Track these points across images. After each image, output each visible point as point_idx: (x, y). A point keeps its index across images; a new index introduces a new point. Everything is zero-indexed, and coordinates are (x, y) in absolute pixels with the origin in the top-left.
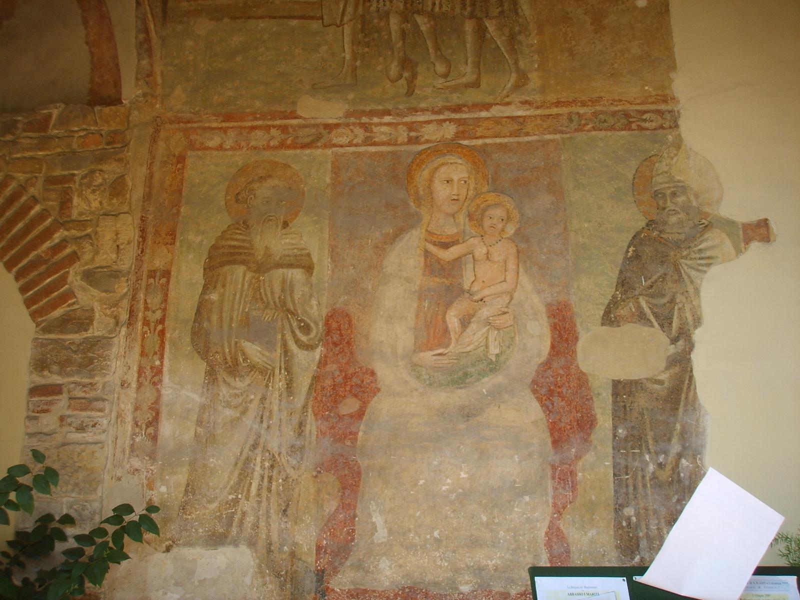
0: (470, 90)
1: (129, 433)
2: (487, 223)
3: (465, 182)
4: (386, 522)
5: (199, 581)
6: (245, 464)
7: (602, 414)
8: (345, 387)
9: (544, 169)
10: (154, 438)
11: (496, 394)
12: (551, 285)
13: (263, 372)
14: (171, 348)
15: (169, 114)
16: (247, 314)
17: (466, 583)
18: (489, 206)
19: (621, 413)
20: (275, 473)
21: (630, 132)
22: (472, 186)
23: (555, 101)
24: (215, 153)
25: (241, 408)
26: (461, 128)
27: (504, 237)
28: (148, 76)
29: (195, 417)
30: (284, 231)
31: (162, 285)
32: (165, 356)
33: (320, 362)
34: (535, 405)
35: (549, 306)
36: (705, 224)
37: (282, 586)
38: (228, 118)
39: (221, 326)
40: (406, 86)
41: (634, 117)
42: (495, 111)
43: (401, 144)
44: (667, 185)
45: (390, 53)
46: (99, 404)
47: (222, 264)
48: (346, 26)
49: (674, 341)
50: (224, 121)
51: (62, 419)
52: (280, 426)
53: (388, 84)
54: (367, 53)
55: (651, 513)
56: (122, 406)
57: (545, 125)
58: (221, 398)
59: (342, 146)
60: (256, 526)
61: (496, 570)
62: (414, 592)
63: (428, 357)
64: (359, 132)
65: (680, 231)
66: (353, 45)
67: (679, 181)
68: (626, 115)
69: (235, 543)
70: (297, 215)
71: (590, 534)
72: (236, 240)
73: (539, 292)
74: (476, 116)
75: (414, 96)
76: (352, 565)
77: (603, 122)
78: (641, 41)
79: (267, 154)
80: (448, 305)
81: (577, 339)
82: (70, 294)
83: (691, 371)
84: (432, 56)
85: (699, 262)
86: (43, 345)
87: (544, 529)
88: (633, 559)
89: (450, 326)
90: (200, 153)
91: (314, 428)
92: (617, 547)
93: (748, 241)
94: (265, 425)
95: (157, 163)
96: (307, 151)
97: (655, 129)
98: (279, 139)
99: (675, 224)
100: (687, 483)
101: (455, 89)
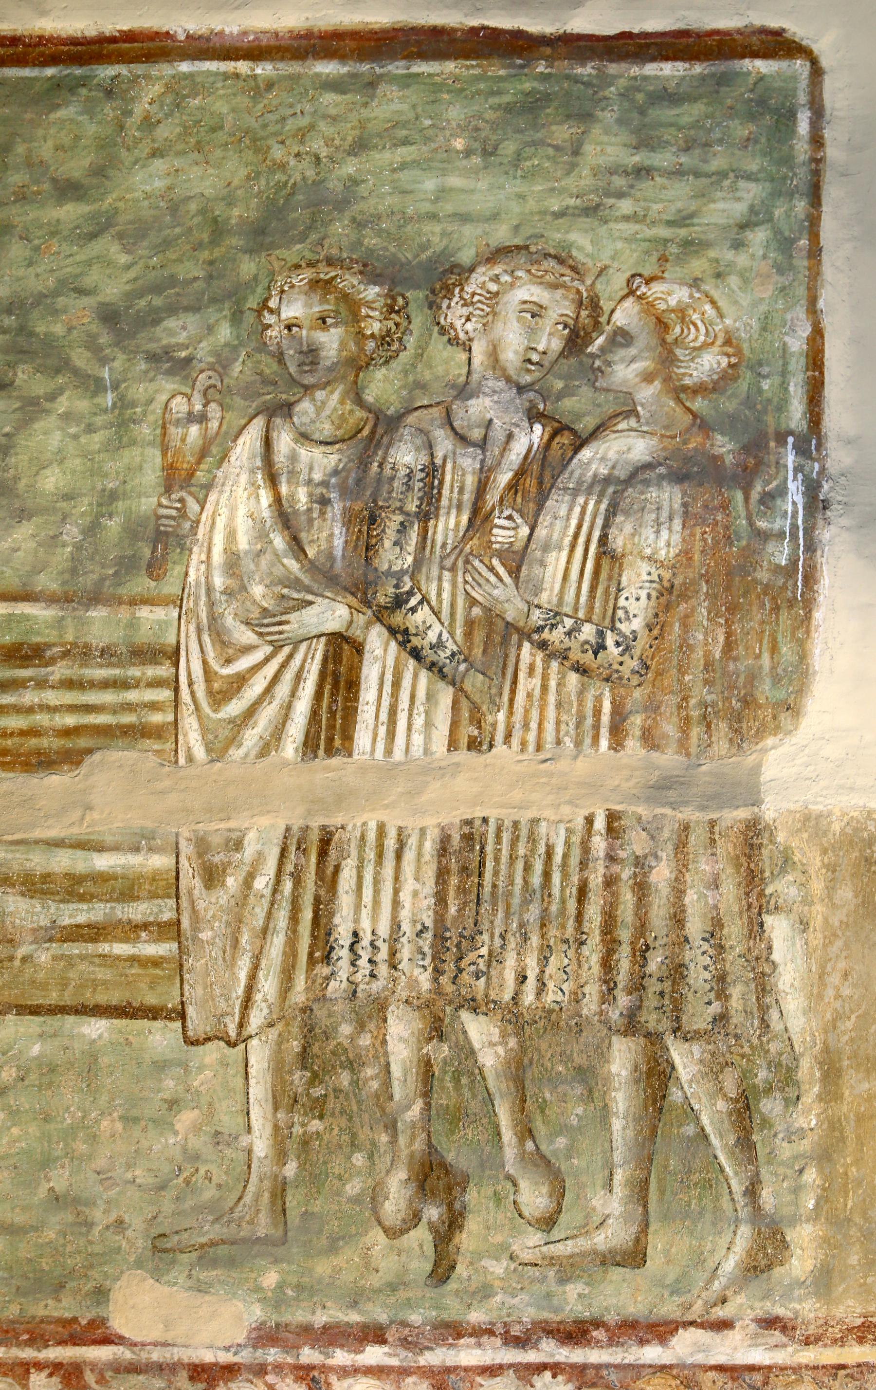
40: (429, 1249)
48: (254, 1042)
53: (377, 1237)
66: (276, 1108)
75: (452, 1285)
84: (510, 1153)
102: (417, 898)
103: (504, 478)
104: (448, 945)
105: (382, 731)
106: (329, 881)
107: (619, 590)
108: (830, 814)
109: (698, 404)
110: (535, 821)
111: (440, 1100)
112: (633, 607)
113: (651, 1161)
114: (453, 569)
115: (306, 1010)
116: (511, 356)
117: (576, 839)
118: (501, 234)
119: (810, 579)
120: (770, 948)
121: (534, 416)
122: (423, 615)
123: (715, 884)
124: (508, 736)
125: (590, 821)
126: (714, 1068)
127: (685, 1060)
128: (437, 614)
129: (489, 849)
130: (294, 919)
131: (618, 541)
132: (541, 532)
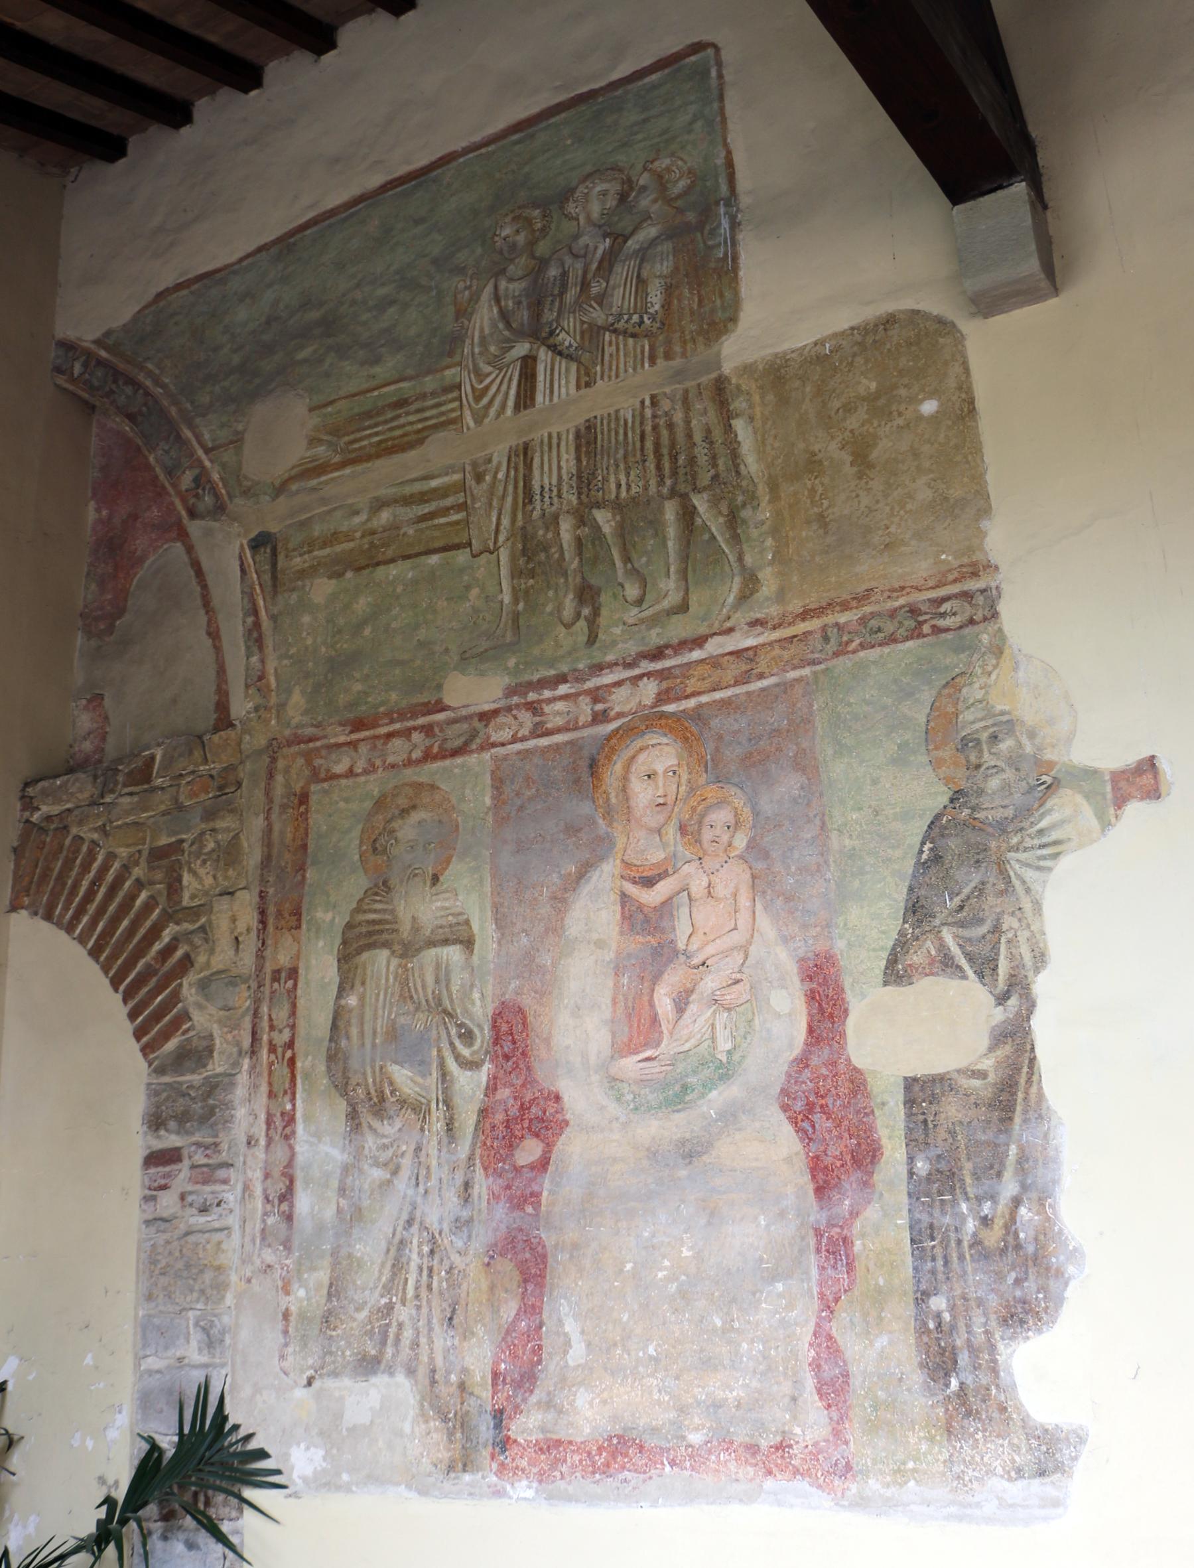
0: (675, 618)
1: (260, 1213)
2: (707, 835)
3: (674, 773)
4: (583, 1332)
5: (347, 1430)
6: (399, 1249)
7: (890, 1138)
8: (523, 1124)
9: (788, 731)
10: (289, 1218)
11: (730, 1116)
12: (805, 926)
13: (416, 1109)
14: (303, 1084)
15: (287, 732)
16: (394, 1022)
17: (697, 1429)
18: (708, 808)
19: (920, 1130)
20: (435, 1262)
21: (920, 641)
22: (685, 777)
23: (801, 610)
24: (344, 782)
25: (392, 1166)
26: (665, 685)
27: (732, 855)
28: (260, 678)
29: (335, 1184)
30: (434, 890)
31: (288, 991)
32: (298, 1096)
33: (487, 1088)
34: (788, 1129)
35: (802, 960)
36: (1046, 783)
37: (451, 1434)
38: (358, 725)
39: (363, 1045)
40: (586, 630)
41: (926, 613)
42: (713, 647)
43: (584, 727)
44: (982, 724)
45: (562, 580)
46: (222, 1173)
47: (359, 951)
49: (1002, 999)
50: (352, 732)
51: (183, 1197)
52: (440, 1189)
53: (561, 631)
54: (532, 586)
55: (973, 1304)
56: (250, 1174)
57: (786, 655)
58: (366, 1151)
59: (503, 745)
60: (415, 1345)
61: (738, 1407)
62: (625, 1443)
63: (630, 1065)
64: (526, 718)
65: (1006, 802)
66: (513, 578)
67: (1003, 713)
68: (913, 611)
69: (391, 1372)
70: (448, 861)
71: (878, 1345)
72: (375, 911)
73: (786, 940)
74: (685, 660)
75: (597, 645)
76: (539, 1403)
77: (876, 633)
78: (931, 476)
79: (409, 774)
80: (656, 978)
81: (846, 1011)
82: (185, 1016)
83: (1033, 1049)
84: (620, 572)
85: (1040, 852)
86: (157, 1093)
87: (808, 1337)
88: (947, 1385)
89: (660, 1012)
90: (325, 785)
91: (484, 1191)
92: (922, 1365)
93: (1120, 802)
94: (421, 1189)
95: (276, 809)
96: (459, 760)
97: (961, 627)
98: (423, 748)
99: (998, 791)
100: (1031, 1249)
101: (654, 621)
102: (568, 461)
103: (594, 266)
104: (585, 480)
105: (548, 391)
106: (529, 466)
107: (647, 295)
108: (756, 362)
109: (679, 203)
110: (617, 411)
111: (587, 555)
112: (654, 300)
113: (688, 557)
114: (574, 312)
115: (523, 528)
116: (595, 215)
117: (637, 413)
118: (589, 169)
119: (735, 259)
120: (736, 436)
121: (605, 235)
122: (563, 335)
123: (705, 412)
124: (602, 378)
125: (643, 402)
126: (715, 502)
127: (700, 503)
128: (568, 333)
129: (598, 430)
130: (516, 487)
131: (645, 274)
132: (612, 282)
